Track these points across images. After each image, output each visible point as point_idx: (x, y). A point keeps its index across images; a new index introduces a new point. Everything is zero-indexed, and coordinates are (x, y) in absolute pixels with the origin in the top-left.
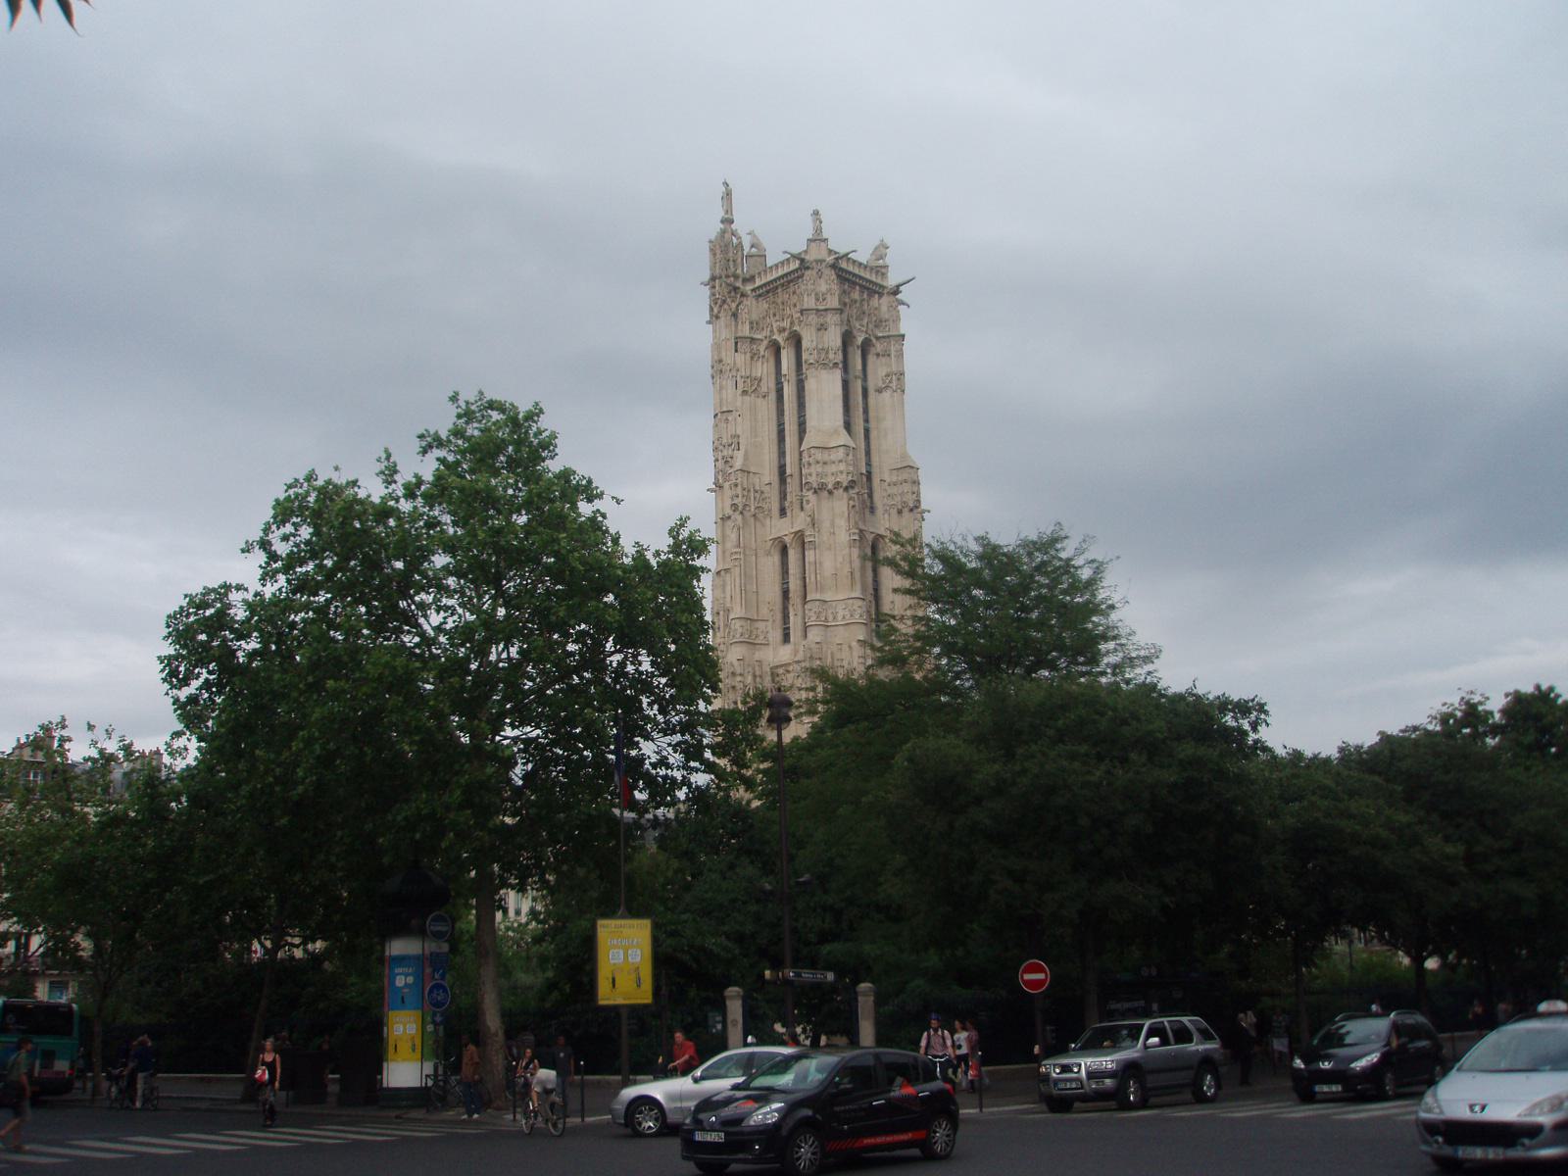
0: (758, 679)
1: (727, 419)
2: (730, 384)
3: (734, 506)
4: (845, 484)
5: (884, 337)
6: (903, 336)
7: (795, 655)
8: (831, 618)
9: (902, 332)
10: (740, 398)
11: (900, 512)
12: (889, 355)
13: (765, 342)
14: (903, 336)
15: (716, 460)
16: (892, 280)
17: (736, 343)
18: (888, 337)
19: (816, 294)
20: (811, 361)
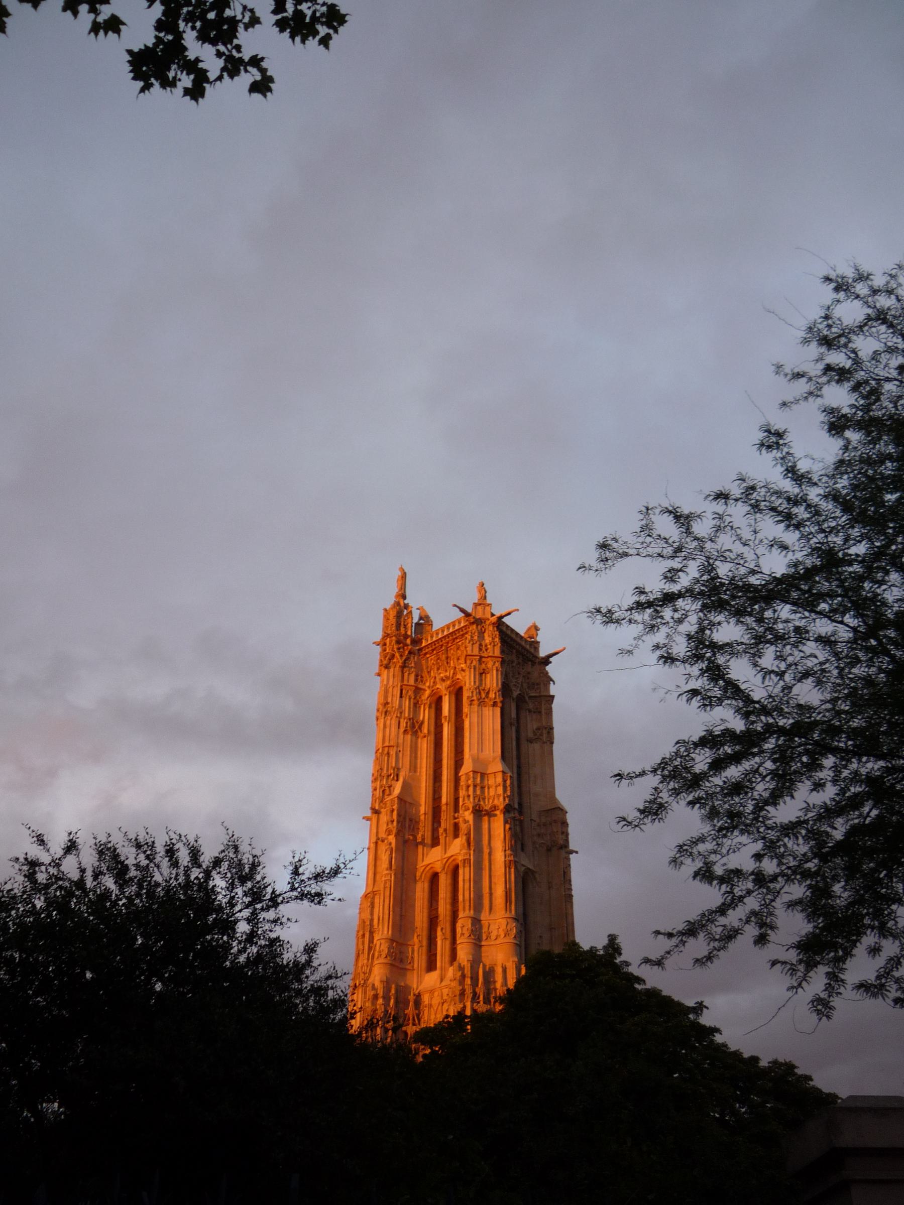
0: (401, 1005)
1: (388, 753)
2: (394, 722)
3: (389, 832)
4: (502, 807)
5: (535, 697)
6: (553, 697)
7: (442, 980)
8: (484, 938)
9: (552, 694)
10: (401, 736)
11: (549, 850)
12: (540, 712)
13: (428, 693)
14: (553, 697)
15: (375, 789)
16: (543, 653)
17: (401, 690)
18: (540, 696)
19: (481, 645)
20: (475, 698)
